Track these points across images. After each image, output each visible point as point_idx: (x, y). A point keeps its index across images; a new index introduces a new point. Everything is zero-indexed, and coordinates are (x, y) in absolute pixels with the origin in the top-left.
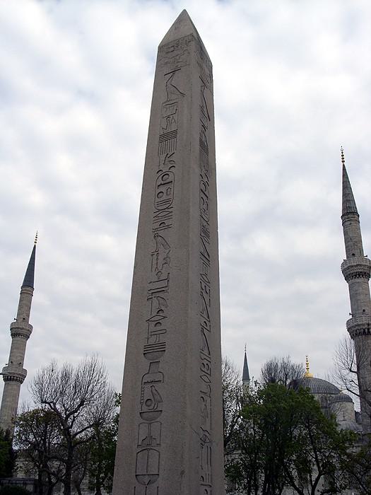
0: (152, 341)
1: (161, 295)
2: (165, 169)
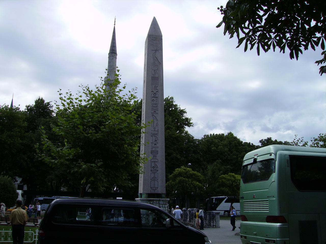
0: (154, 149)
1: (156, 135)
2: (155, 92)
